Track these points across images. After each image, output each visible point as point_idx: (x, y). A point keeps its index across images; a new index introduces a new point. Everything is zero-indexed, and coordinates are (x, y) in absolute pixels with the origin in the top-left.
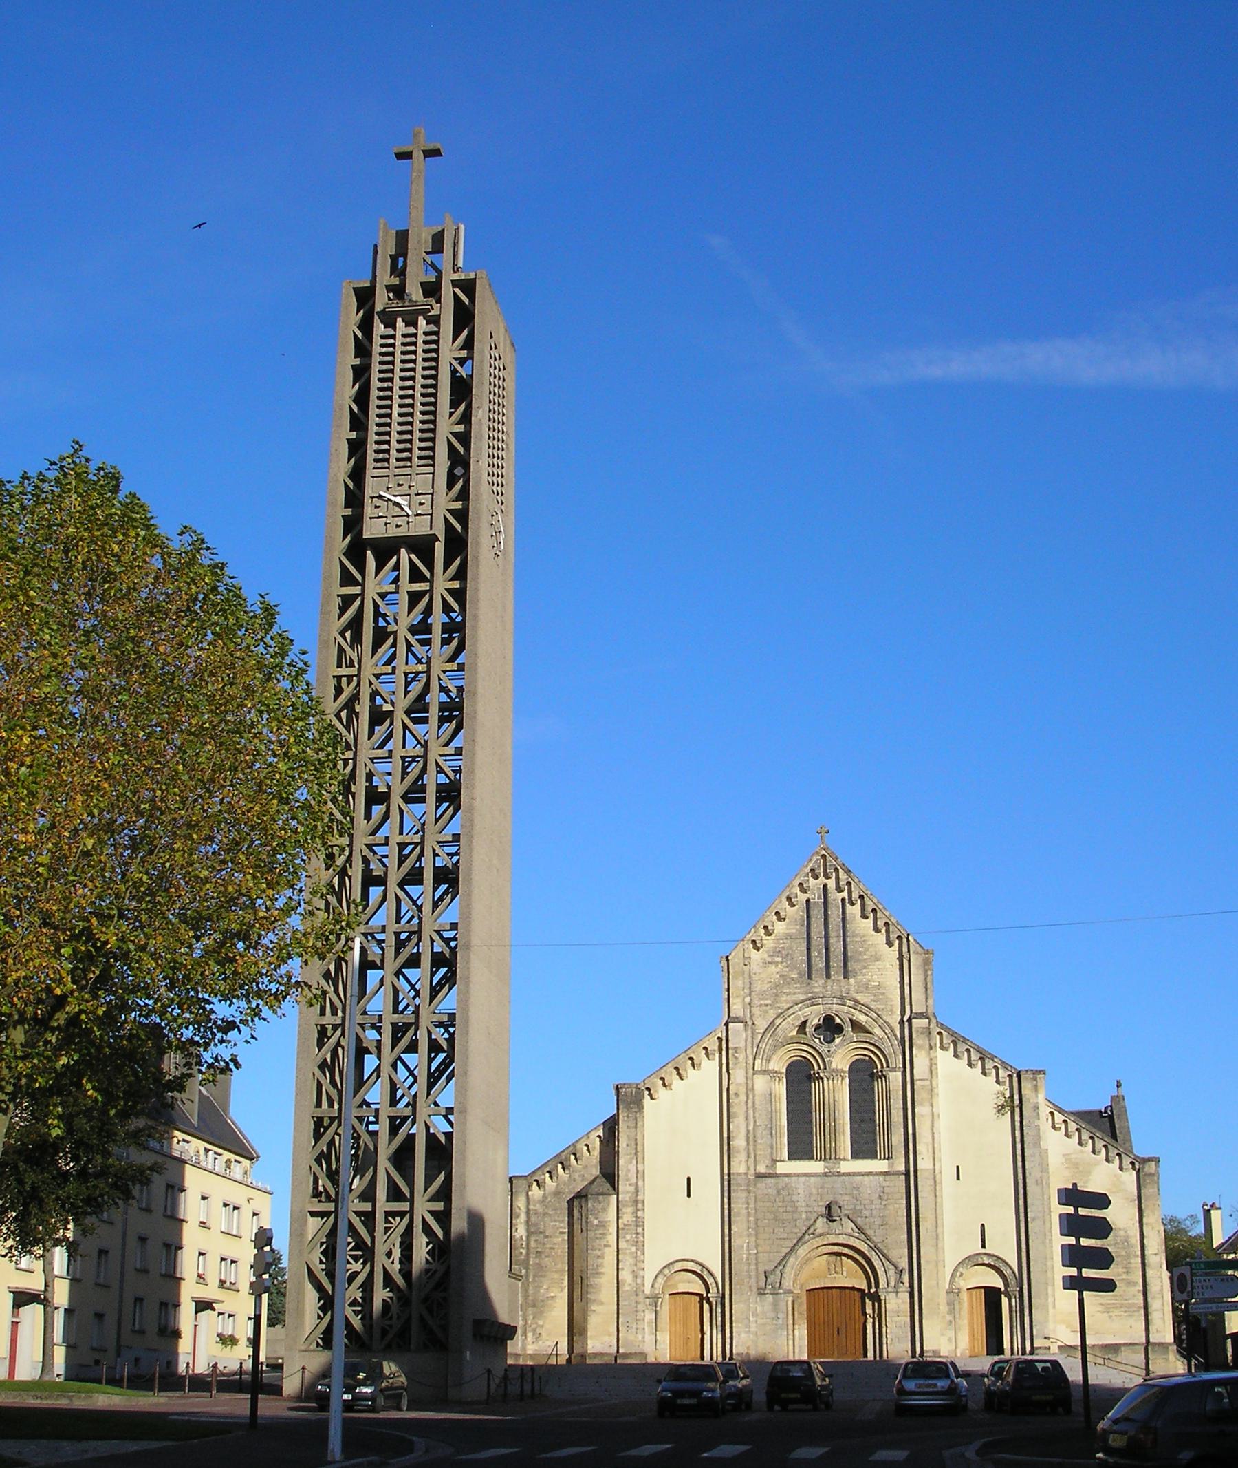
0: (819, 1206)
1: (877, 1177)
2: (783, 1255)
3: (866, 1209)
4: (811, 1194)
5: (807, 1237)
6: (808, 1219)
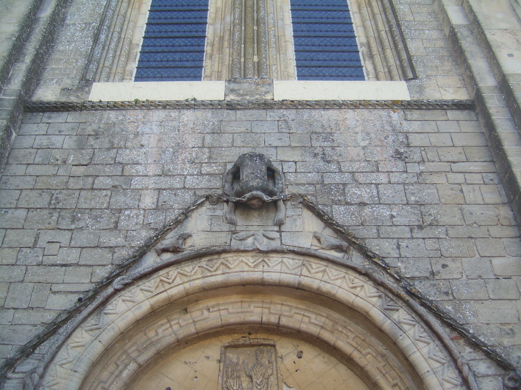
2: (49, 317)
4: (179, 147)
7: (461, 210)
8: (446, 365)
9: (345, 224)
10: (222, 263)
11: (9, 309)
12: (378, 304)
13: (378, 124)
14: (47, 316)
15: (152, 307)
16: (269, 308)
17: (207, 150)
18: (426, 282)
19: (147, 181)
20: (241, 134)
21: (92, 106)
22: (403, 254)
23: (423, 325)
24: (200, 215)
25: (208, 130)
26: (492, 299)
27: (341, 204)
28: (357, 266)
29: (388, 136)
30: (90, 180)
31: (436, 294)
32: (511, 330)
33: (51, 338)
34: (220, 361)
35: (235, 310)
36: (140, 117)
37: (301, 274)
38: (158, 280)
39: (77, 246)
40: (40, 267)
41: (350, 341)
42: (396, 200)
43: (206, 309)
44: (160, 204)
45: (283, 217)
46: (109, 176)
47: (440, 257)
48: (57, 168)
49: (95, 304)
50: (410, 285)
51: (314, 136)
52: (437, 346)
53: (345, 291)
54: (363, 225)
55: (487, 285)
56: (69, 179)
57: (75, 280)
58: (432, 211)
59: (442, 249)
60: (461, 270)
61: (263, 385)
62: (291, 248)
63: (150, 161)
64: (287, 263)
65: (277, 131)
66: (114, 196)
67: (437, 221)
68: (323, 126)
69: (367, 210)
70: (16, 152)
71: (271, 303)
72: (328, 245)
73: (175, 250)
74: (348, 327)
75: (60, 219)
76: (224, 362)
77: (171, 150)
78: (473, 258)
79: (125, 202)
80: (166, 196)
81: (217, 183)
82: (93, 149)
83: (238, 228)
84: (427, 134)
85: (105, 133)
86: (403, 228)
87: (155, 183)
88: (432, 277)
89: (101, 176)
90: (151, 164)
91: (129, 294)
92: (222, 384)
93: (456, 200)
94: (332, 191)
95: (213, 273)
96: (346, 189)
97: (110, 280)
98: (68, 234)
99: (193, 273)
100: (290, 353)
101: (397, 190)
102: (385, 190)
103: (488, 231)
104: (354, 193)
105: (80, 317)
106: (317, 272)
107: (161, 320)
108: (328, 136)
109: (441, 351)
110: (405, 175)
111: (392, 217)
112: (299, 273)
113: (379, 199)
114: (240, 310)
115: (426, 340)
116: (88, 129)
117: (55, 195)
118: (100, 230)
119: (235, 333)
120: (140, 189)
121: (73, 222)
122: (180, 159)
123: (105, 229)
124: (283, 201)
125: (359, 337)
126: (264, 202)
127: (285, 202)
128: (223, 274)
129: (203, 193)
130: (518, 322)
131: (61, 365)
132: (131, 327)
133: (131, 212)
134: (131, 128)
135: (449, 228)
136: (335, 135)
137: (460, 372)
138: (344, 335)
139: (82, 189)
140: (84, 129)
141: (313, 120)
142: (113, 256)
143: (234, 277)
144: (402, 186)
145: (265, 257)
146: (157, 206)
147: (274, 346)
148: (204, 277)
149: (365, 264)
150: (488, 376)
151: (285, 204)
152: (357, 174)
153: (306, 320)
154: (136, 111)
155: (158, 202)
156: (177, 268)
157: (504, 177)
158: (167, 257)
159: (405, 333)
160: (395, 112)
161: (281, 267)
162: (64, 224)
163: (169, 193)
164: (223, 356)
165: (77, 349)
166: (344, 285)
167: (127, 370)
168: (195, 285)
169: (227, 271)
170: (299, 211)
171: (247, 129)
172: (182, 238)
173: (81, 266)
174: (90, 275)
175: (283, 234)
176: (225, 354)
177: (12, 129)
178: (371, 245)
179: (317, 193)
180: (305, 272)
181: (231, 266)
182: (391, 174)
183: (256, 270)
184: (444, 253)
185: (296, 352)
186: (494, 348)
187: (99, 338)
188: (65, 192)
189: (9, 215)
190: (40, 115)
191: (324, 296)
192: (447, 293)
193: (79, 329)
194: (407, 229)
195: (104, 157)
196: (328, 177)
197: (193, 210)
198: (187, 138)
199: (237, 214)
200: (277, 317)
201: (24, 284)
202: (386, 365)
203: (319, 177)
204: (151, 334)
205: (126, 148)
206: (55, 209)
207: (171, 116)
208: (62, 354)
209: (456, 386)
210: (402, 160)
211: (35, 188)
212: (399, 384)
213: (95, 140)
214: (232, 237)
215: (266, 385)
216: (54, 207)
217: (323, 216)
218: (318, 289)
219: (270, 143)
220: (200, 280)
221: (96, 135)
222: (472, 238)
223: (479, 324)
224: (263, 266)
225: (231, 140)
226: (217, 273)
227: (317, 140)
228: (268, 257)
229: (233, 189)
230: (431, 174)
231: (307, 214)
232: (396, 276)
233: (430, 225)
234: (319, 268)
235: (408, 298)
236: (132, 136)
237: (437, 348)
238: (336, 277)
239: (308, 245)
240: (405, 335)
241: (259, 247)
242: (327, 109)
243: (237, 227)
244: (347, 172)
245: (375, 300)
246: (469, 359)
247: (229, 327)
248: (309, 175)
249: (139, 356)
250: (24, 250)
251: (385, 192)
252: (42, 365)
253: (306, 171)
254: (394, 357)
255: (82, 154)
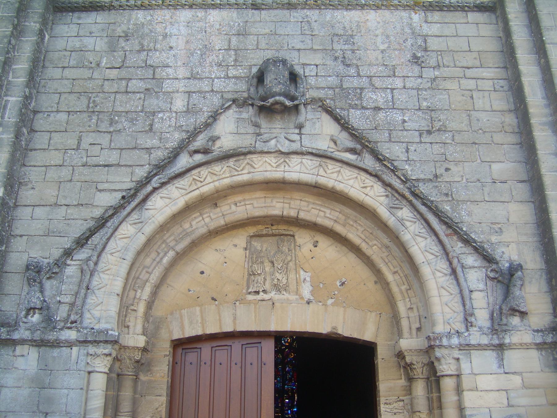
0: (227, 77)
1: (404, 14)
2: (98, 213)
3: (375, 89)
4: (207, 49)
5: (184, 161)
6: (189, 111)
7: (469, 116)
8: (439, 257)
9: (360, 127)
10: (248, 164)
11: (61, 205)
12: (385, 203)
13: (398, 26)
14: (95, 212)
15: (186, 203)
16: (289, 204)
17: (233, 53)
18: (429, 183)
19: (177, 84)
20: (266, 36)
21: (120, 6)
22: (411, 157)
23: (423, 222)
24: (227, 118)
25: (234, 32)
26: (486, 201)
27: (357, 109)
28: (368, 168)
29: (407, 40)
30: (124, 83)
31: (437, 195)
32: (500, 229)
33: (101, 231)
34: (246, 249)
35: (259, 205)
36: (168, 17)
37: (318, 174)
38: (191, 179)
39: (117, 147)
40: (85, 167)
41: (359, 234)
42: (409, 106)
43: (234, 204)
44: (190, 107)
45: (303, 120)
46: (141, 79)
47: (444, 161)
48: (91, 71)
49: (137, 201)
50: (415, 187)
51: (336, 39)
52: (433, 241)
53: (356, 190)
54: (376, 129)
55: (484, 188)
56: (104, 82)
57: (118, 179)
58: (442, 117)
59: (447, 154)
60: (462, 173)
61: (283, 270)
62: (310, 150)
63: (179, 63)
64: (306, 164)
65: (300, 33)
66: (147, 99)
67: (445, 127)
68: (345, 28)
69: (381, 115)
70: (50, 55)
71: (291, 199)
72: (343, 148)
73: (206, 151)
74: (358, 222)
75: (99, 122)
76: (250, 249)
77: (199, 52)
78: (475, 163)
79: (157, 105)
80: (195, 99)
81: (242, 86)
82: (124, 51)
83: (262, 131)
84: (445, 38)
85: (135, 34)
86: (413, 133)
87: (185, 86)
88: (435, 179)
89: (134, 79)
90: (180, 66)
91: (165, 192)
92: (248, 269)
93: (466, 107)
94: (350, 95)
95: (240, 173)
96: (363, 94)
97: (148, 179)
98: (107, 137)
99: (222, 172)
100: (307, 242)
101: (411, 95)
102: (399, 94)
103: (492, 137)
104: (370, 97)
105: (125, 212)
106: (333, 173)
107: (195, 213)
108: (349, 38)
109: (436, 245)
110: (419, 80)
111: (404, 121)
112: (316, 173)
113: (393, 104)
114: (263, 205)
115: (424, 235)
116: (118, 30)
117: (92, 99)
118: (137, 132)
119: (259, 225)
120: (171, 92)
121: (111, 124)
122: (208, 62)
123: (141, 132)
124: (304, 105)
125: (367, 231)
126: (286, 107)
127: (306, 106)
128: (248, 173)
129: (230, 96)
130: (507, 222)
131: (111, 254)
132: (169, 221)
133: (164, 114)
134: (159, 28)
135: (455, 134)
136: (356, 37)
137: (451, 264)
138: (354, 229)
139: (117, 92)
140: (114, 30)
141: (335, 21)
142: (149, 157)
143: (259, 176)
144: (416, 91)
145: (286, 157)
146: (188, 109)
147: (293, 236)
148: (232, 176)
149: (376, 166)
150: (474, 267)
151: (306, 108)
152: (374, 78)
153: (322, 214)
154: (163, 11)
155: (188, 104)
156: (207, 168)
157: (514, 84)
158: (199, 158)
159: (406, 229)
160: (416, 13)
161: (301, 168)
162: (104, 126)
163: (198, 96)
164: (249, 244)
165: (124, 240)
166: (356, 185)
167: (167, 257)
168: (224, 183)
169: (253, 170)
170: (318, 114)
171: (271, 31)
172: (212, 140)
173: (122, 166)
174: (130, 174)
175: (303, 136)
176: (250, 242)
177: (45, 31)
178: (383, 148)
179: (335, 97)
180: (322, 172)
181: (256, 166)
182: (407, 79)
183: (278, 170)
184: (448, 157)
185: (312, 241)
186: (483, 244)
187: (142, 231)
188: (101, 95)
189: (51, 118)
190: (70, 15)
191: (338, 194)
192: (447, 195)
193: (124, 223)
194: (417, 133)
195: (135, 59)
196: (347, 81)
197: (221, 113)
198: (213, 40)
199: (261, 117)
200: (297, 211)
201: (73, 183)
202: (389, 255)
203: (338, 81)
204: (186, 226)
205: (156, 50)
206: (93, 112)
207: (198, 16)
208: (112, 245)
209: (446, 275)
210: (419, 65)
211: (73, 91)
212: (399, 271)
213: (125, 41)
214: (256, 139)
215: (286, 270)
216: (92, 110)
217: (340, 120)
218: (333, 188)
219: (293, 45)
220: (229, 179)
221: (126, 36)
222: (476, 144)
223: (472, 223)
224: (285, 166)
225: (256, 43)
226: (243, 172)
227: (339, 42)
228: (289, 158)
229: (258, 92)
230: (445, 80)
231: (326, 118)
232: (402, 178)
233: (439, 130)
234: (334, 168)
235: (411, 198)
236: (160, 38)
237: (433, 243)
238: (350, 177)
239: (325, 147)
240: (406, 230)
241: (281, 149)
242: (350, 9)
243: (261, 130)
244: (365, 77)
245: (382, 199)
246: (460, 252)
247: (254, 219)
248: (329, 79)
249: (176, 245)
250: (69, 152)
251: (399, 97)
252: (96, 254)
253: (326, 75)
254: (396, 249)
255: (114, 57)
